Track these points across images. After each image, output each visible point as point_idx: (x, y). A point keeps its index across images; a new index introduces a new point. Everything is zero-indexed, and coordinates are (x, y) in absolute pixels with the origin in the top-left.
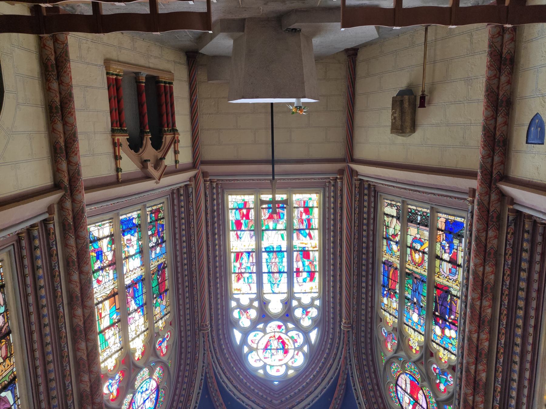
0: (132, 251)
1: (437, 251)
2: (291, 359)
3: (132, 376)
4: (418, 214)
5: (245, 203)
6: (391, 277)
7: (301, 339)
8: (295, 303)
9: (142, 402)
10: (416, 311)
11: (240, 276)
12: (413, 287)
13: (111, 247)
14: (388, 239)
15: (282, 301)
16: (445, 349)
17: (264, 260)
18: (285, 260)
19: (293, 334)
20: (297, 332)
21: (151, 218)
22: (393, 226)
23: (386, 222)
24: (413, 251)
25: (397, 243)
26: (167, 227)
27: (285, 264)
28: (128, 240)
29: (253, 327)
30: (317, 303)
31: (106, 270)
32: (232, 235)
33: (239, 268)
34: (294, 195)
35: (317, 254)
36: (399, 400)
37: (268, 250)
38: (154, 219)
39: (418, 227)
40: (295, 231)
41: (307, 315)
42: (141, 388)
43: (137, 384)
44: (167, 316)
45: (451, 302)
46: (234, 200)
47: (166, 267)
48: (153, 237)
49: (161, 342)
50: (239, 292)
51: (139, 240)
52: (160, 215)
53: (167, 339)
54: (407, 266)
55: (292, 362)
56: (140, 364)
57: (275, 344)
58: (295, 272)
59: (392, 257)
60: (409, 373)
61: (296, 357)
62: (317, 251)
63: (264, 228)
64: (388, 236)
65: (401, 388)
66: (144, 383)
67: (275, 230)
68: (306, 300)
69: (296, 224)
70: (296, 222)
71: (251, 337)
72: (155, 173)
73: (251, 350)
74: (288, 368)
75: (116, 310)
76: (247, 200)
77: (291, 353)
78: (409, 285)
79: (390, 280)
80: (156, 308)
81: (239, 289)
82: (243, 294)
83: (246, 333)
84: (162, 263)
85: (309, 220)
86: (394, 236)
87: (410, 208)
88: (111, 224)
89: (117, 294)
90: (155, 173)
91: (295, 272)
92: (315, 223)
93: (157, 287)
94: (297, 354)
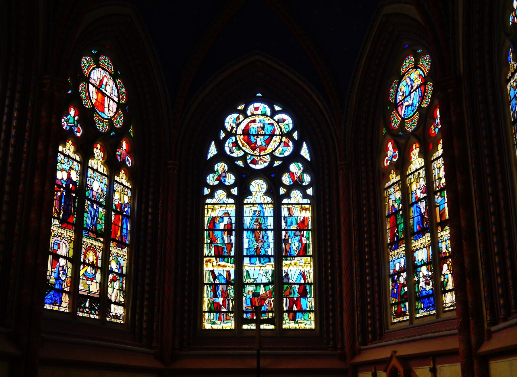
0: (424, 270)
1: (71, 267)
2: (240, 123)
3: (421, 128)
4: (88, 308)
5: (294, 319)
6: (120, 228)
8: (234, 191)
9: (412, 94)
10: (94, 194)
11: (302, 226)
12: (97, 220)
13: (444, 279)
14: (121, 275)
15: (250, 194)
16: (68, 156)
17: (272, 245)
18: (246, 246)
19: (237, 154)
20: (233, 155)
21: (405, 306)
22: (115, 291)
23: (122, 296)
24: (95, 263)
25: (112, 272)
26: (388, 293)
27: (246, 240)
28: (429, 284)
29: (287, 161)
30: (207, 191)
31: (449, 253)
32: (311, 279)
33: (303, 236)
34: (233, 328)
35: (206, 252)
36: (116, 86)
37: (267, 260)
38: (403, 306)
39: (89, 293)
40: (233, 282)
41: (220, 176)
42: (413, 111)
43: (417, 115)
44: (388, 185)
45: (60, 210)
46: (308, 323)
47: (389, 245)
48: (403, 283)
49: (394, 157)
50: (303, 206)
51: (418, 282)
52: (396, 309)
53: (387, 158)
54: (101, 245)
55: (239, 119)
56: (413, 139)
58: (234, 230)
59: (118, 253)
60: (105, 120)
61: (234, 125)
62: (206, 257)
63: (271, 287)
64: (121, 279)
65: (114, 101)
66: (411, 115)
67: (258, 285)
68: (220, 195)
69: (231, 291)
70: (232, 294)
72: (395, 362)
73: (289, 135)
74: (244, 112)
75: (439, 206)
76: (291, 322)
77: (239, 131)
78: (101, 222)
79: (120, 225)
80: (399, 198)
81: (303, 210)
82: (298, 204)
83: (295, 157)
84: (394, 250)
85: (215, 296)
86: (114, 280)
87: (97, 315)
88: (444, 305)
89: (439, 224)
90: (395, 362)
91: (234, 230)
92: (207, 293)
93: (398, 223)
94: (233, 128)
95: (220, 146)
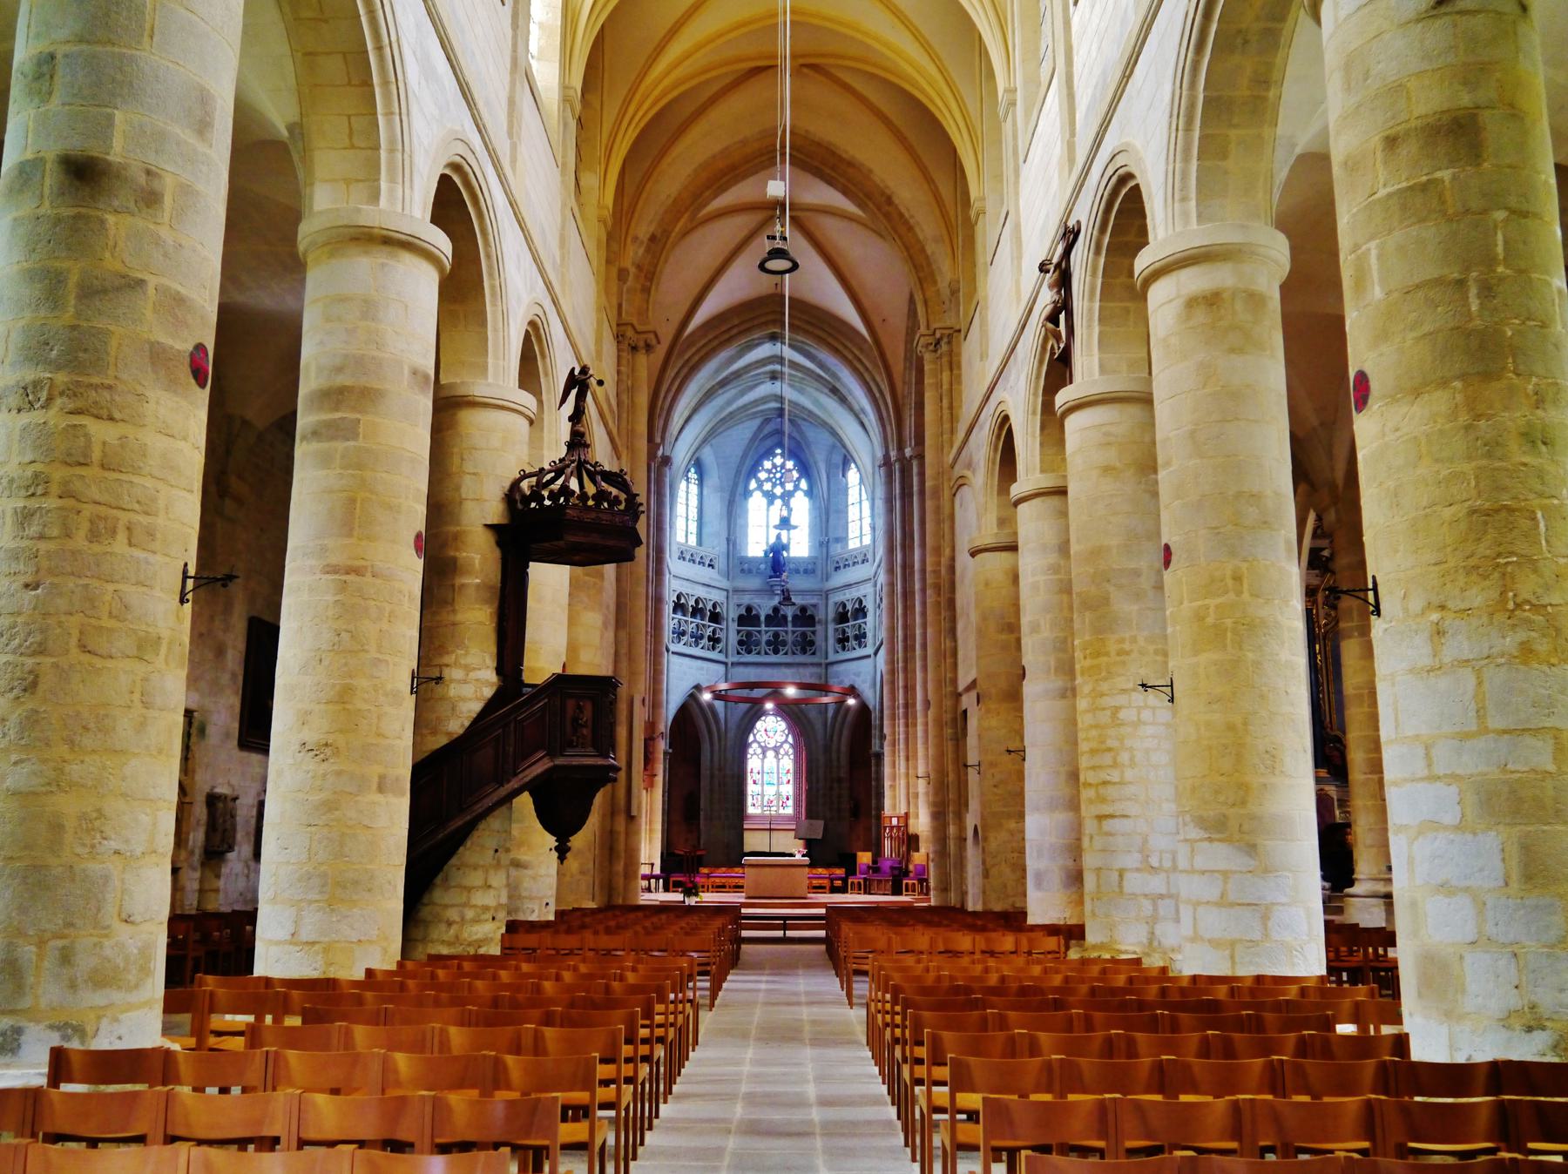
7: (758, 737)
8: (761, 756)
11: (788, 772)
29: (782, 743)
30: (749, 756)
57: (771, 734)
71: (783, 739)
77: (763, 730)
83: (786, 741)
95: (755, 735)
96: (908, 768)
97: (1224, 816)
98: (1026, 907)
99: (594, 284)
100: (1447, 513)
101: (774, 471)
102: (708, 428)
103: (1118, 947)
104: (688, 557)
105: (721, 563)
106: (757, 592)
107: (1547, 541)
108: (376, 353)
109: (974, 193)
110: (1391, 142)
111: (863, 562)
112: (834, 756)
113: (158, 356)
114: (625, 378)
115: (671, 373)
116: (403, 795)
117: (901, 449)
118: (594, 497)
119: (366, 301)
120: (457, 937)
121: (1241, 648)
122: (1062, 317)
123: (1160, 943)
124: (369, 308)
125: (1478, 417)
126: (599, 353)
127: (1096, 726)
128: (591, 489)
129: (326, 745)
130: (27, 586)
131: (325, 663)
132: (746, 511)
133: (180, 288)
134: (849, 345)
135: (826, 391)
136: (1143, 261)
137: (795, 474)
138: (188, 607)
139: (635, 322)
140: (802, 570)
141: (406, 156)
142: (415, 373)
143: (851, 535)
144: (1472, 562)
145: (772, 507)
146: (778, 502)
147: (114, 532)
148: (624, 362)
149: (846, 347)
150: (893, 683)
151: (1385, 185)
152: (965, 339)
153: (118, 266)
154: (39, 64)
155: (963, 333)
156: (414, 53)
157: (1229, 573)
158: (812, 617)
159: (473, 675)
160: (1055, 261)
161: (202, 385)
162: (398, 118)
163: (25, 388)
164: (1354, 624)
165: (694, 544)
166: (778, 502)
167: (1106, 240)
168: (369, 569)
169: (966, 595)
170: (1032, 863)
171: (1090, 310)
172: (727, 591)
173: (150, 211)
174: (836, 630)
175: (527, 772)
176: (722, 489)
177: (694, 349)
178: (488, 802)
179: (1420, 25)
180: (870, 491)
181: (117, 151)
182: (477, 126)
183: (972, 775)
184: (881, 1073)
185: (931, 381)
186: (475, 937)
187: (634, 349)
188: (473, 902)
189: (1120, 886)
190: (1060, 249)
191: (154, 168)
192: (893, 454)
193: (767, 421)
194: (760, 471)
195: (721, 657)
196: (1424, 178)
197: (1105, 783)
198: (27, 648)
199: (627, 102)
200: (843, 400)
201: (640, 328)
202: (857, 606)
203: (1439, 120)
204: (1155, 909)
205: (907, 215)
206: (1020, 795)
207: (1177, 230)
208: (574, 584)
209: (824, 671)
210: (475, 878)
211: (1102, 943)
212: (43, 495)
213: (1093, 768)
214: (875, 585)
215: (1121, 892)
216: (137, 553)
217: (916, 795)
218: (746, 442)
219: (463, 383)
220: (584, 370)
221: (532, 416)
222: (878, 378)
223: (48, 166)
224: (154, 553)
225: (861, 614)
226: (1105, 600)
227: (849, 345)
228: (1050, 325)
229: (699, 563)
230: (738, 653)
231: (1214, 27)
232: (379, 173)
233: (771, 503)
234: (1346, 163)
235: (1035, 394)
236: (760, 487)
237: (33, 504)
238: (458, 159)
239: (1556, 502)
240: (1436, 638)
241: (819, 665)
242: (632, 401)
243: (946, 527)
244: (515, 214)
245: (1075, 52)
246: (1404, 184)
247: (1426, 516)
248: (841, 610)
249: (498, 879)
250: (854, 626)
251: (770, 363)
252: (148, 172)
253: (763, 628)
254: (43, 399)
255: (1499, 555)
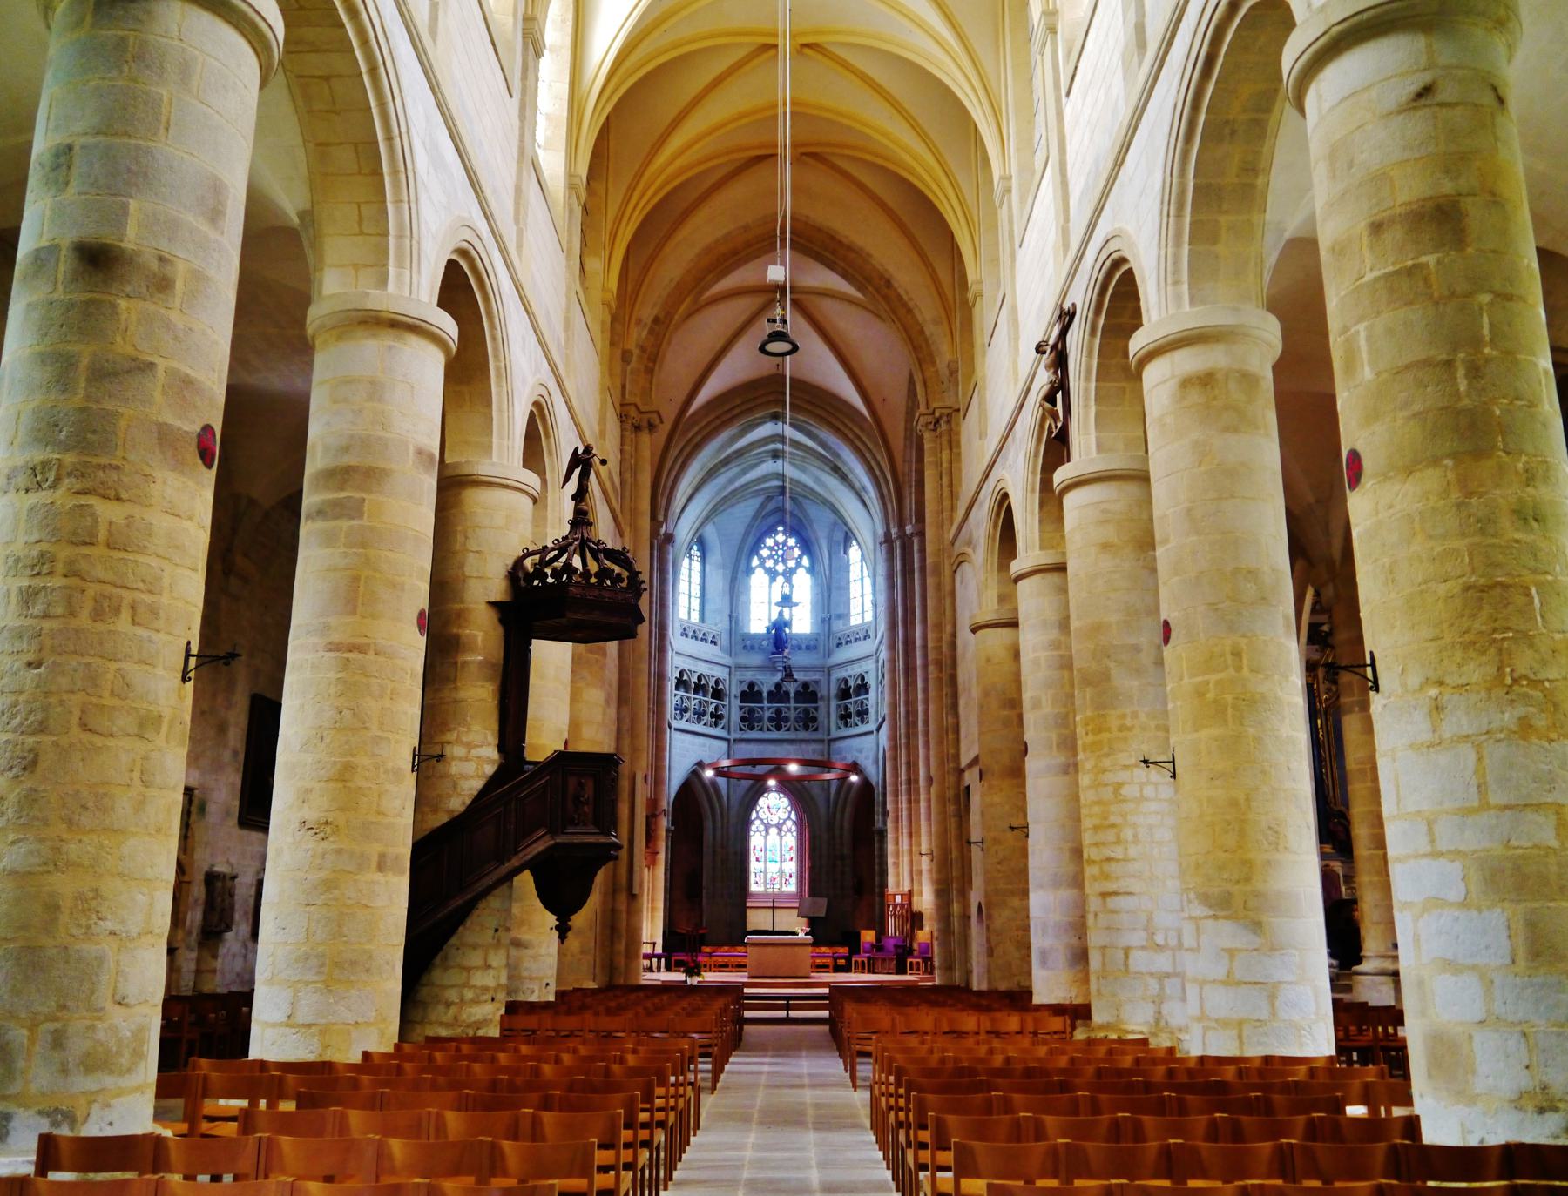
7: (761, 813)
8: (764, 833)
11: (791, 849)
29: (785, 820)
30: (752, 833)
57: (773, 811)
71: (786, 815)
73: (786, 808)
83: (789, 818)
95: (757, 812)
96: (911, 845)
97: (1230, 894)
98: (1031, 986)
99: (598, 367)
100: (1442, 589)
101: (776, 548)
102: (710, 507)
103: (1124, 1027)
104: (691, 634)
105: (723, 640)
106: (760, 668)
107: (1542, 617)
108: (381, 434)
109: (971, 277)
110: (1377, 228)
111: (865, 639)
112: (837, 832)
113: (165, 437)
114: (627, 456)
115: (674, 452)
116: (403, 873)
117: (901, 526)
118: (596, 575)
119: (373, 383)
120: (456, 1018)
121: (1242, 725)
122: (1059, 396)
123: (1167, 1023)
124: (376, 389)
125: (1470, 494)
126: (602, 434)
127: (1099, 802)
128: (593, 567)
129: (326, 823)
130: (29, 665)
131: (327, 740)
132: (748, 588)
133: (189, 371)
134: (850, 424)
135: (827, 469)
136: (1138, 343)
137: (797, 552)
138: (190, 685)
139: (639, 404)
140: (804, 647)
141: (414, 242)
142: (420, 452)
143: (853, 612)
144: (1467, 638)
145: (774, 584)
146: (780, 579)
147: (118, 610)
148: (628, 441)
149: (846, 426)
150: (895, 759)
151: (1371, 270)
152: (964, 418)
153: (129, 350)
154: (57, 156)
155: (962, 413)
156: (424, 143)
157: (1228, 649)
158: (814, 694)
159: (474, 752)
160: (1051, 342)
161: (209, 465)
162: (406, 206)
163: (33, 469)
164: (1355, 699)
165: (697, 621)
166: (780, 579)
167: (1101, 321)
168: (372, 647)
169: (967, 672)
170: (1037, 941)
171: (1087, 390)
172: (730, 667)
173: (161, 296)
174: (839, 706)
175: (529, 849)
176: (723, 567)
177: (696, 429)
178: (489, 881)
179: (1401, 117)
180: (871, 568)
181: (131, 238)
182: (485, 213)
183: (976, 851)
184: (886, 1158)
185: (931, 459)
186: (473, 1019)
187: (637, 428)
188: (473, 982)
189: (1126, 964)
190: (1056, 331)
191: (167, 255)
192: (894, 531)
193: (769, 499)
194: (762, 548)
195: (723, 734)
196: (1410, 263)
197: (1109, 860)
198: (29, 726)
199: (631, 189)
200: (844, 478)
201: (643, 408)
202: (859, 682)
203: (1423, 206)
204: (1162, 988)
205: (905, 298)
206: (1023, 873)
207: (1170, 312)
208: (577, 661)
209: (826, 746)
210: (475, 959)
211: (1108, 1023)
212: (48, 574)
213: (1096, 844)
214: (877, 661)
215: (1127, 971)
216: (139, 631)
217: (920, 872)
218: (748, 520)
219: (467, 462)
220: (588, 449)
221: (536, 494)
222: (879, 458)
223: (64, 252)
224: (158, 631)
225: (863, 691)
226: (1105, 676)
227: (850, 424)
228: (1047, 405)
229: (702, 640)
230: (741, 730)
231: (1202, 118)
232: (388, 259)
233: (773, 579)
234: (1333, 249)
235: (1034, 472)
236: (762, 564)
237: (38, 582)
238: (465, 245)
239: (1549, 578)
240: (1435, 712)
241: (822, 741)
242: (635, 480)
243: (948, 601)
244: (521, 297)
245: (1068, 142)
246: (1391, 269)
247: (1422, 592)
248: (843, 686)
249: (497, 959)
250: (856, 702)
251: (773, 442)
252: (161, 259)
253: (766, 704)
254: (51, 479)
255: (1495, 630)
